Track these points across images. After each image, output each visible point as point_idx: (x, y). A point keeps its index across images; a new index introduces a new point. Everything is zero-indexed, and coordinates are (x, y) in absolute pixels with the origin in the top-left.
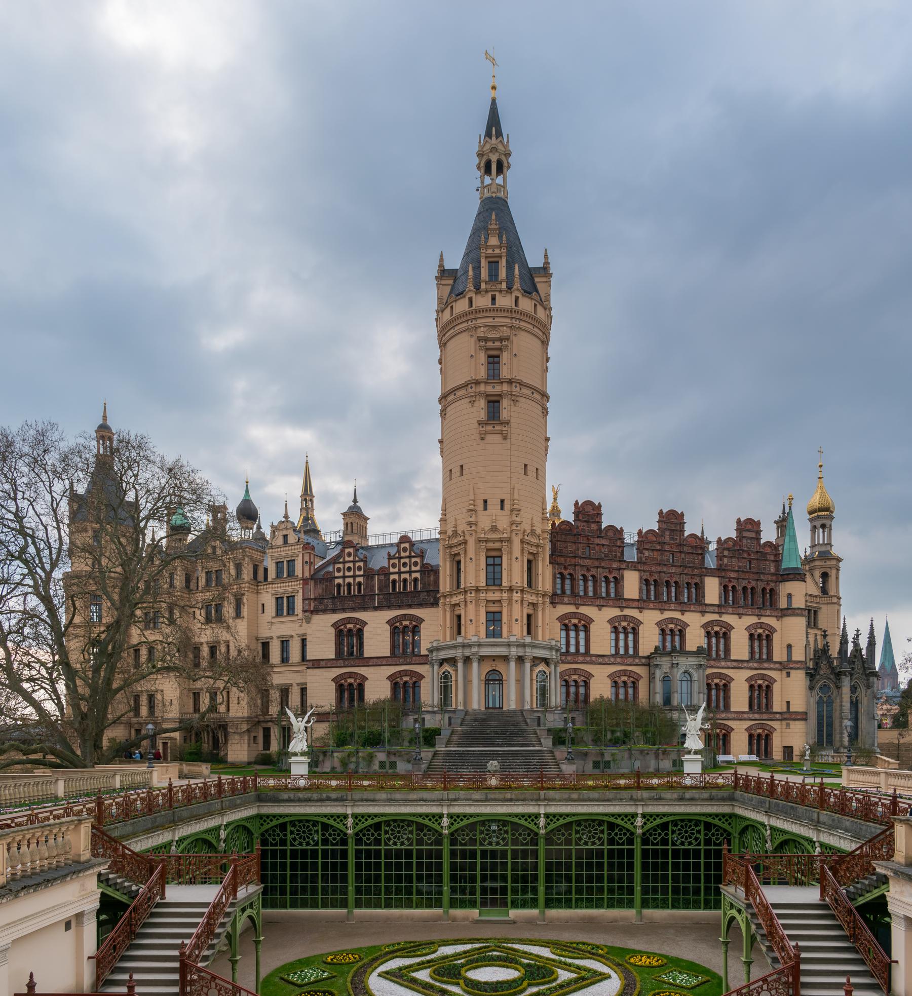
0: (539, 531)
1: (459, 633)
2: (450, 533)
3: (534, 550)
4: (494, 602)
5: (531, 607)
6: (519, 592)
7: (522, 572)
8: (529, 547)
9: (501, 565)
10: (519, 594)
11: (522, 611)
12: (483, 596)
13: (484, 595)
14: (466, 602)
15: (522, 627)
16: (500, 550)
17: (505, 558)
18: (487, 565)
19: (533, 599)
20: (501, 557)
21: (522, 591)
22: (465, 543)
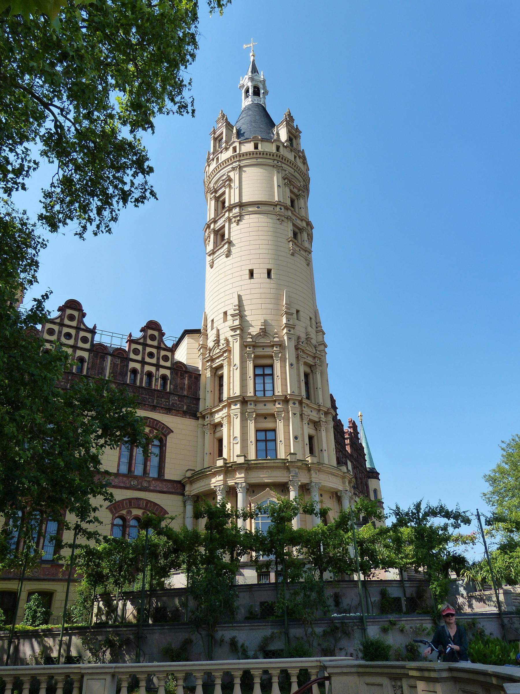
0: (314, 342)
1: (220, 454)
2: (210, 344)
3: (310, 361)
4: (265, 416)
5: (312, 426)
6: (297, 403)
7: (299, 381)
8: (305, 356)
9: (272, 375)
10: (297, 405)
11: (302, 428)
12: (250, 407)
13: (252, 406)
14: (229, 416)
15: (304, 447)
16: (272, 357)
17: (277, 365)
18: (255, 375)
19: (314, 416)
20: (271, 366)
21: (301, 403)
22: (229, 351)
